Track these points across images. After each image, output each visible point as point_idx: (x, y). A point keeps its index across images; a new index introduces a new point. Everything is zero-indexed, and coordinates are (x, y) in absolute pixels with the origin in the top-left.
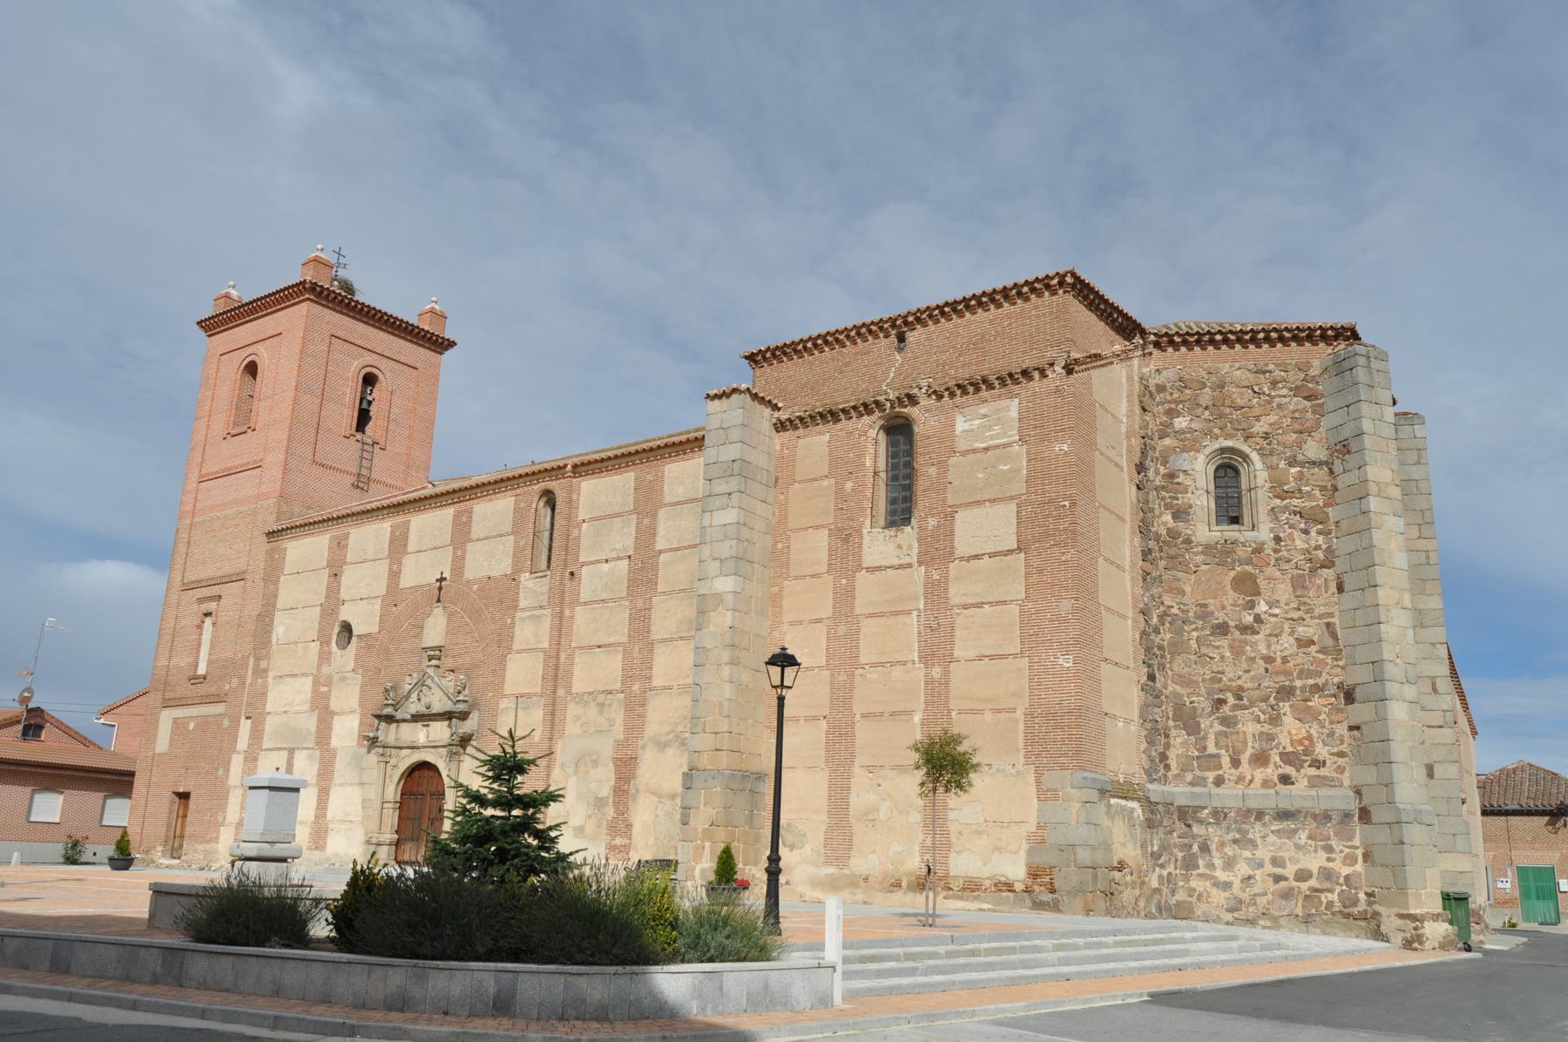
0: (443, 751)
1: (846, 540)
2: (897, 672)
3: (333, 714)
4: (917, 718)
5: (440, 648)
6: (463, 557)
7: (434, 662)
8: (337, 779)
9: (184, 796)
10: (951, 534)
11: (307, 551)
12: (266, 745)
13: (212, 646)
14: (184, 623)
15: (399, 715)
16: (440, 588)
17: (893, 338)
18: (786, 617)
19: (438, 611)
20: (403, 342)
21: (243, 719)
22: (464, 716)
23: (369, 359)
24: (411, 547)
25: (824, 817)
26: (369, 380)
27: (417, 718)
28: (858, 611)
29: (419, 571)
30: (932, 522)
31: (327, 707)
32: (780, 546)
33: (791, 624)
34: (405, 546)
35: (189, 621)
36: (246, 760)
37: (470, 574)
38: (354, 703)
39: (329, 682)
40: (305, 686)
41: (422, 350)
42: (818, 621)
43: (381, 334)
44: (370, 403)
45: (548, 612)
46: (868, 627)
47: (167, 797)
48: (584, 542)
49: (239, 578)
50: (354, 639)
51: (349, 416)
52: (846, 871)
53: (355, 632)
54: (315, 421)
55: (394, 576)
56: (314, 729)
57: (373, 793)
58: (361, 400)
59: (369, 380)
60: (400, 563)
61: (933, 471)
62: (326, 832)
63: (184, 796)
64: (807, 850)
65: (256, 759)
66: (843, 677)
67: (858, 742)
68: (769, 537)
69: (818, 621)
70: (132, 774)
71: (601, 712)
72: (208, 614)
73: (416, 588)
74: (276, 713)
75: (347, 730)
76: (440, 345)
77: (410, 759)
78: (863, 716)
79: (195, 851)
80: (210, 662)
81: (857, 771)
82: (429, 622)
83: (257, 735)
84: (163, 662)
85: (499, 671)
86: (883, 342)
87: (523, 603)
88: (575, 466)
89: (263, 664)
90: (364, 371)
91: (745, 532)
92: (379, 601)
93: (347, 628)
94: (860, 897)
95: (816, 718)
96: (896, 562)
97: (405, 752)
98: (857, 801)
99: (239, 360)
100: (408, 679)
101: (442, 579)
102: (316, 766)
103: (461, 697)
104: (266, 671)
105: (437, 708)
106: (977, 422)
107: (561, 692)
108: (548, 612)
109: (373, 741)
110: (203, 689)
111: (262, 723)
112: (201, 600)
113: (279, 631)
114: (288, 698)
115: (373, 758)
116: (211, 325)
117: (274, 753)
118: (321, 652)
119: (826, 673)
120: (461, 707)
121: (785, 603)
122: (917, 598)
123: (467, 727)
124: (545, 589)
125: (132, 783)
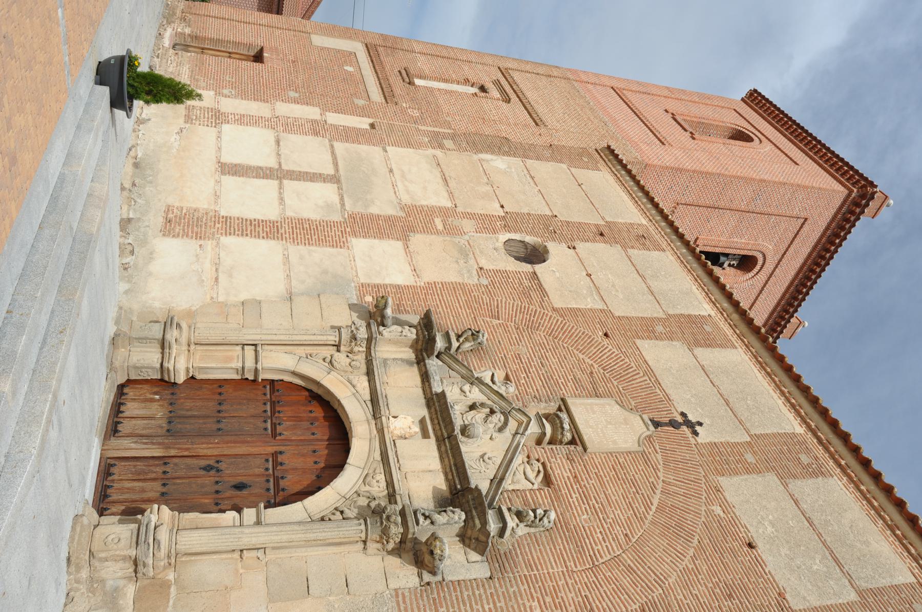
0: (379, 488)
3: (405, 239)
5: (577, 440)
6: (750, 470)
8: (295, 251)
9: (258, 58)
12: (337, 145)
13: (447, 92)
14: (466, 68)
16: (673, 424)
20: (778, 296)
21: (371, 121)
22: (474, 539)
24: (706, 355)
27: (437, 405)
31: (412, 229)
34: (698, 344)
36: (314, 122)
38: (431, 275)
39: (451, 231)
40: (435, 196)
47: (259, 42)
50: (527, 267)
53: (539, 268)
54: (722, 204)
55: (648, 328)
56: (374, 210)
57: (274, 324)
58: (726, 255)
62: (198, 236)
63: (258, 58)
65: (316, 133)
72: (483, 89)
73: (649, 371)
74: (387, 159)
75: (384, 264)
79: (180, 64)
80: (431, 90)
82: (610, 407)
84: (417, 48)
89: (448, 143)
97: (363, 384)
100: (500, 375)
102: (315, 216)
103: (512, 521)
104: (441, 146)
105: (469, 450)
109: (376, 316)
111: (370, 141)
112: (497, 83)
113: (499, 163)
114: (412, 175)
115: (344, 317)
116: (755, 99)
117: (329, 157)
118: (490, 217)
125: (270, 11)
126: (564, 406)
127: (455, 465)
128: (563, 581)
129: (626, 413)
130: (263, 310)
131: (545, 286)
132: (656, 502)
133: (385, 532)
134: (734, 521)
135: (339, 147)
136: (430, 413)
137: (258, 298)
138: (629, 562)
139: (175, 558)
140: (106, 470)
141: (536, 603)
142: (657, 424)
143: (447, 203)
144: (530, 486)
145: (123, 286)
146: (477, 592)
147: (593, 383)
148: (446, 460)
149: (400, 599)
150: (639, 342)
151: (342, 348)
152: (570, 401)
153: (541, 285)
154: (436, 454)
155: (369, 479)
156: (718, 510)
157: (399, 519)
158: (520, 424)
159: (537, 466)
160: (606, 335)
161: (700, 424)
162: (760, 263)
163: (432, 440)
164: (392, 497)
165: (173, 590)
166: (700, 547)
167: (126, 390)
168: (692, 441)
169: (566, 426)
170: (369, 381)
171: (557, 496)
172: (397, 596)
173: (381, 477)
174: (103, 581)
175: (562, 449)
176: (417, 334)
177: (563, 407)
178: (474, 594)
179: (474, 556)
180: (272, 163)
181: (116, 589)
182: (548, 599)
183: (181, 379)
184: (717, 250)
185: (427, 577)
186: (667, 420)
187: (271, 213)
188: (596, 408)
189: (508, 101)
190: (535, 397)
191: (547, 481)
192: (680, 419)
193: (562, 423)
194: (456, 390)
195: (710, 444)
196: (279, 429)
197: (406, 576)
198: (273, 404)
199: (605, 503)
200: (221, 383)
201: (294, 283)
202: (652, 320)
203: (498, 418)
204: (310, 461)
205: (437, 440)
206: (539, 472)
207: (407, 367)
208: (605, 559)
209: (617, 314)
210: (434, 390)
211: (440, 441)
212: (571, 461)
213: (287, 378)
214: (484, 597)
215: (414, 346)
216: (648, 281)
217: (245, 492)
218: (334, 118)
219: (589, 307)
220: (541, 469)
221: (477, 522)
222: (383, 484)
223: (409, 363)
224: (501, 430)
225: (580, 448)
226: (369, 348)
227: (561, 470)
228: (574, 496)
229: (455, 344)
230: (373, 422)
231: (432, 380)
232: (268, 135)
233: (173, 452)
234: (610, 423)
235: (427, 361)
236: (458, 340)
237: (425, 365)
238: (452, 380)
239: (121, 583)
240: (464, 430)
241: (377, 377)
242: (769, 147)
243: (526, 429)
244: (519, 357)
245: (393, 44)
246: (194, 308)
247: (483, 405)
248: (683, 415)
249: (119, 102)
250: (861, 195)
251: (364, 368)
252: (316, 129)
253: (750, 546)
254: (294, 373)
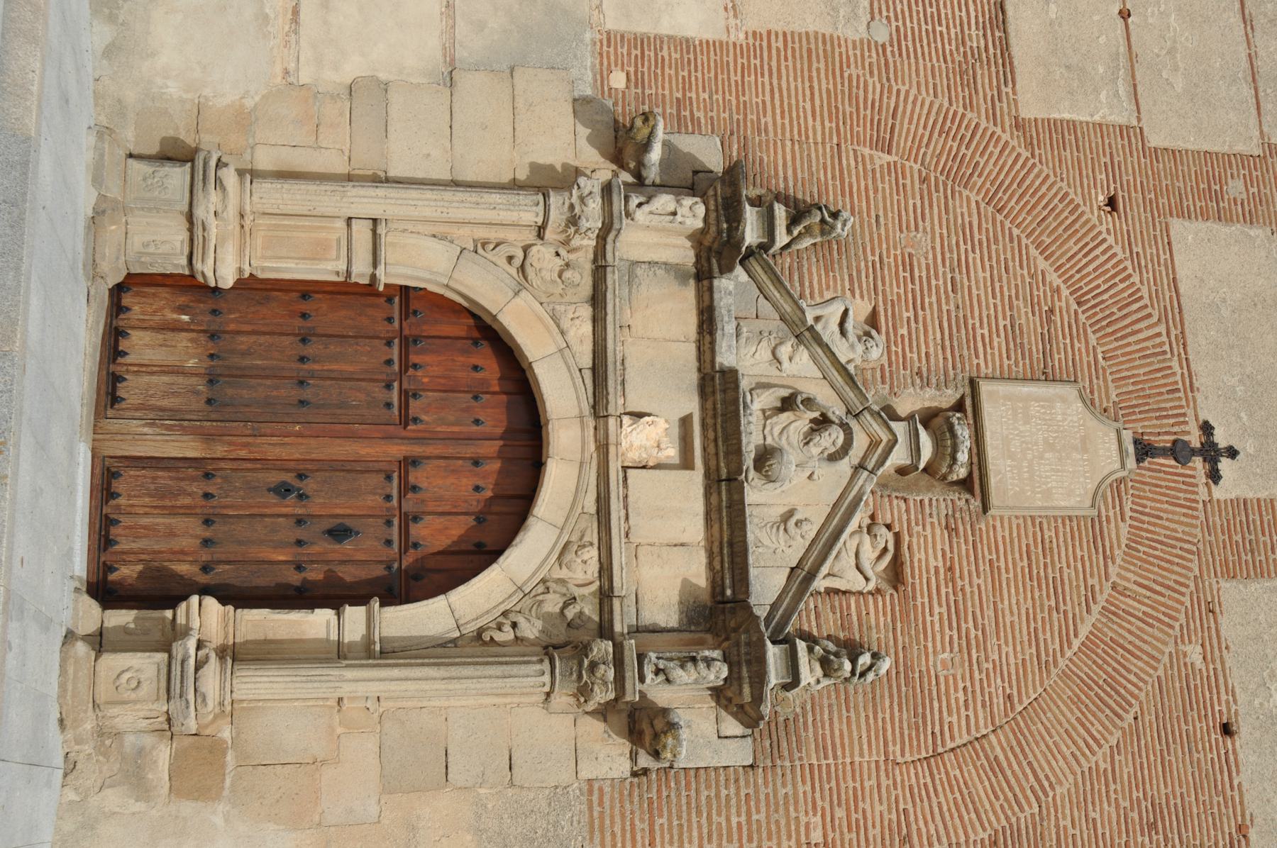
0: (585, 568)
5: (974, 484)
15: (732, 286)
16: (1179, 451)
19: (1106, 452)
27: (719, 391)
60: (1250, 219)
82: (1065, 405)
92: (1122, 116)
101: (1211, 453)
103: (809, 673)
115: (565, 142)
126: (970, 405)
127: (731, 544)
128: (874, 782)
129: (1092, 423)
130: (394, 111)
131: (1016, 50)
132: (1084, 631)
133: (584, 692)
134: (1217, 679)
136: (703, 408)
137: (383, 76)
138: (998, 750)
139: (231, 711)
140: (106, 480)
141: (819, 818)
142: (1144, 450)
144: (857, 583)
145: (99, 35)
146: (724, 792)
147: (1047, 339)
148: (716, 527)
149: (595, 798)
150: (1177, 225)
151: (548, 234)
152: (985, 388)
153: (1005, 47)
154: (699, 507)
155: (570, 556)
156: (1194, 654)
157: (611, 674)
158: (873, 444)
159: (885, 537)
160: (1112, 202)
161: (1232, 453)
163: (695, 479)
164: (606, 595)
165: (230, 757)
166: (1136, 731)
167: (127, 300)
168: (1202, 490)
169: (963, 457)
170: (594, 320)
171: (906, 612)
172: (591, 792)
173: (592, 554)
174: (118, 735)
175: (941, 501)
176: (706, 220)
177: (968, 402)
178: (718, 796)
179: (732, 726)
181: (141, 752)
182: (840, 813)
183: (228, 281)
185: (645, 761)
186: (1165, 441)
188: (1035, 408)
190: (919, 373)
191: (896, 574)
192: (1195, 439)
193: (955, 450)
194: (764, 353)
195: (1235, 503)
196: (415, 407)
197: (611, 757)
198: (407, 343)
199: (990, 629)
200: (306, 290)
201: (462, 28)
202: (1228, 159)
203: (832, 438)
204: (467, 482)
205: (707, 475)
206: (885, 550)
207: (675, 287)
208: (959, 742)
209: (1155, 141)
210: (718, 359)
211: (713, 482)
212: (951, 530)
214: (733, 802)
215: (697, 239)
216: (1259, 39)
217: (348, 546)
219: (1097, 118)
220: (891, 547)
221: (747, 690)
222: (593, 568)
223: (677, 272)
224: (833, 458)
225: (976, 504)
226: (602, 238)
227: (926, 555)
228: (937, 610)
229: (782, 238)
230: (591, 423)
231: (719, 334)
233: (220, 450)
234: (1050, 447)
235: (716, 282)
236: (789, 231)
237: (711, 289)
238: (760, 325)
239: (148, 740)
240: (765, 457)
241: (610, 318)
243: (881, 462)
244: (908, 263)
246: (249, 103)
247: (809, 402)
248: (1207, 428)
251: (586, 288)
253: (1227, 730)
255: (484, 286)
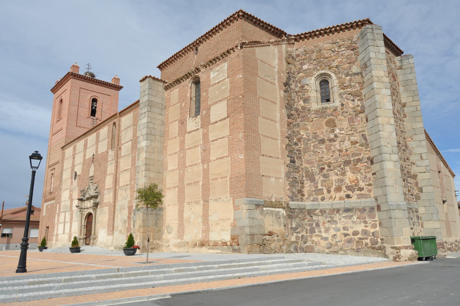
1: (183, 124)
2: (195, 168)
4: (200, 184)
5: (92, 177)
7: (92, 181)
8: (74, 220)
9: (48, 227)
10: (209, 116)
11: (69, 151)
15: (85, 199)
17: (195, 50)
18: (168, 153)
23: (94, 94)
24: (88, 147)
25: (177, 222)
26: (94, 100)
28: (186, 148)
29: (89, 154)
30: (204, 112)
32: (167, 129)
33: (169, 155)
35: (49, 177)
37: (99, 152)
40: (68, 192)
41: (112, 90)
42: (176, 153)
43: (97, 86)
44: (96, 107)
45: (114, 161)
46: (188, 153)
47: (45, 227)
48: (123, 137)
49: (58, 163)
51: (88, 111)
52: (183, 241)
54: (76, 114)
55: (85, 156)
58: (92, 107)
59: (94, 100)
61: (204, 94)
63: (48, 227)
64: (173, 233)
66: (182, 172)
67: (186, 194)
68: (162, 127)
69: (176, 153)
70: (39, 222)
71: (125, 192)
76: (119, 88)
77: (86, 212)
78: (187, 185)
80: (53, 188)
81: (186, 205)
83: (60, 209)
84: (45, 189)
85: (104, 182)
86: (192, 52)
87: (109, 160)
88: (120, 113)
90: (92, 98)
91: (151, 125)
93: (76, 173)
94: (186, 250)
95: (175, 187)
96: (195, 128)
97: (86, 210)
98: (186, 215)
99: (58, 100)
101: (94, 155)
106: (216, 73)
107: (117, 187)
108: (114, 161)
110: (52, 196)
112: (51, 170)
113: (64, 176)
114: (65, 195)
116: (54, 90)
119: (178, 171)
120: (96, 194)
121: (168, 148)
122: (200, 140)
123: (98, 200)
124: (113, 154)
135: (61, 211)
143: (69, 191)
162: (94, 97)
180: (63, 224)
184: (90, 111)
187: (69, 224)
189: (54, 169)
197: (99, 206)
213: (86, 221)
218: (57, 212)
232: (60, 225)
242: (63, 94)
245: (45, 196)
249: (46, 248)
250: (73, 75)
252: (59, 216)
254: (85, 220)
255: (84, 217)
